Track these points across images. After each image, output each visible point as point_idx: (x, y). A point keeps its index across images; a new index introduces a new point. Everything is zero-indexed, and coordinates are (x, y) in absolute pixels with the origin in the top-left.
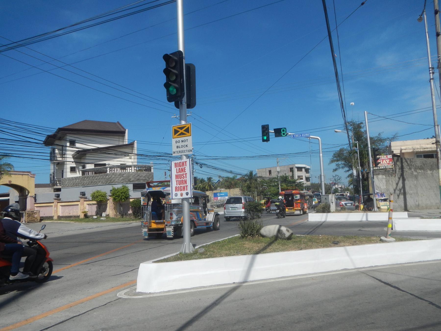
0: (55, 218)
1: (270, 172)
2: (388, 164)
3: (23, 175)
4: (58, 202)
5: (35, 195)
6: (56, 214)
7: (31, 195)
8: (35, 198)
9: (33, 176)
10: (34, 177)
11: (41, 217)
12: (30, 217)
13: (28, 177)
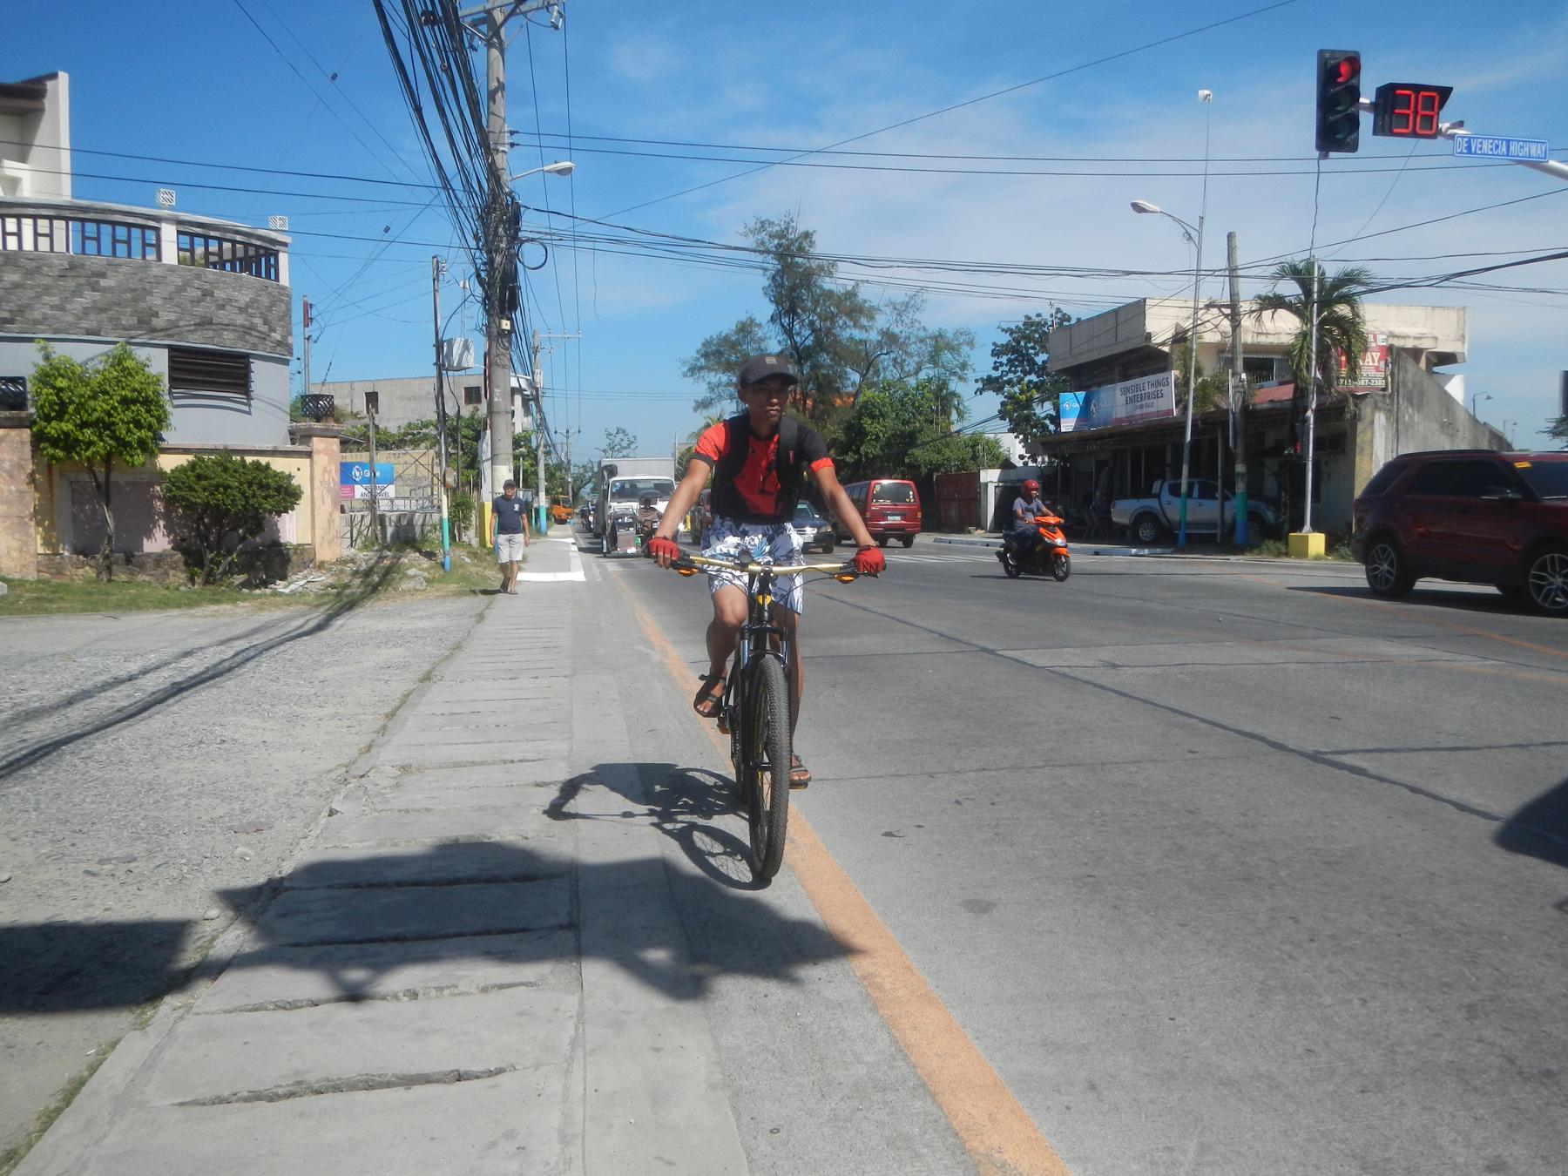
1: (372, 398)
2: (1377, 369)
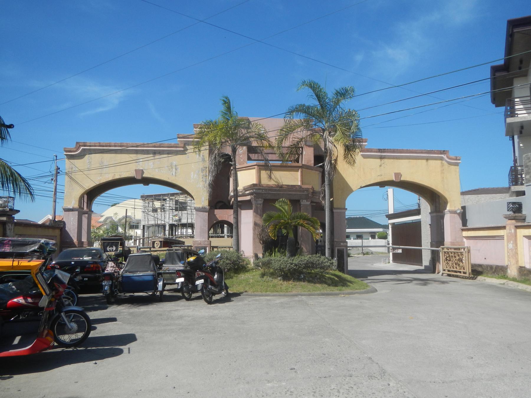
0: (513, 272)
3: (427, 159)
4: (517, 227)
5: (464, 208)
6: (513, 261)
7: (453, 209)
8: (463, 215)
9: (455, 162)
10: (457, 164)
11: (473, 266)
12: (450, 263)
13: (443, 165)
